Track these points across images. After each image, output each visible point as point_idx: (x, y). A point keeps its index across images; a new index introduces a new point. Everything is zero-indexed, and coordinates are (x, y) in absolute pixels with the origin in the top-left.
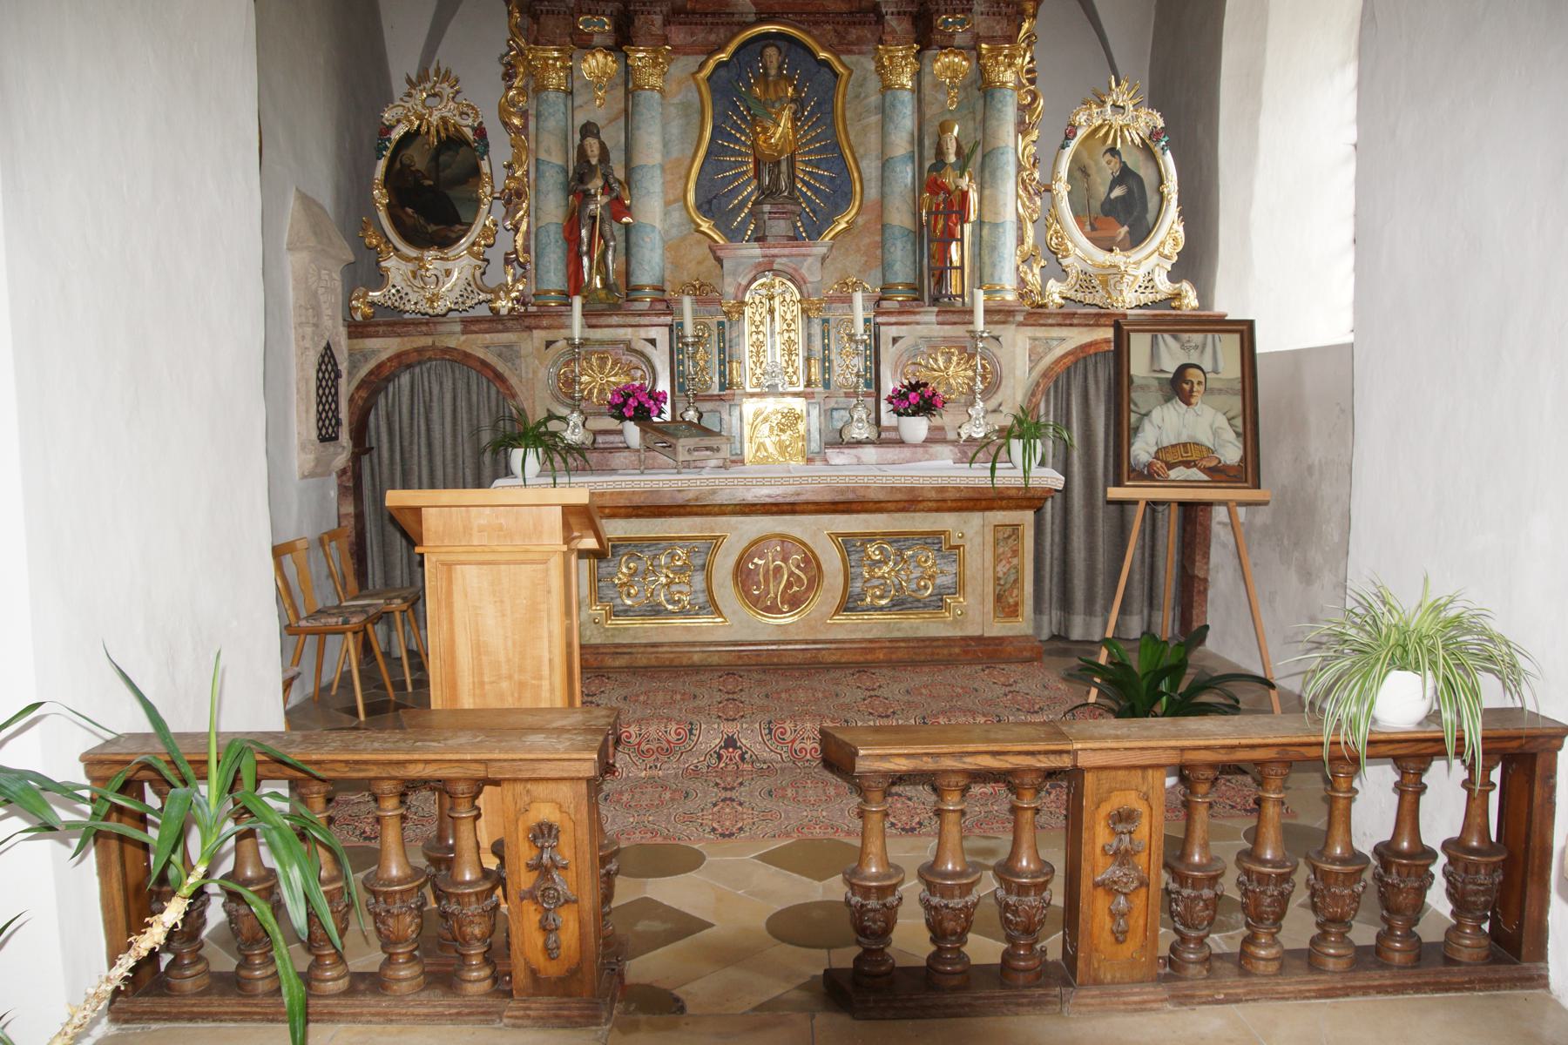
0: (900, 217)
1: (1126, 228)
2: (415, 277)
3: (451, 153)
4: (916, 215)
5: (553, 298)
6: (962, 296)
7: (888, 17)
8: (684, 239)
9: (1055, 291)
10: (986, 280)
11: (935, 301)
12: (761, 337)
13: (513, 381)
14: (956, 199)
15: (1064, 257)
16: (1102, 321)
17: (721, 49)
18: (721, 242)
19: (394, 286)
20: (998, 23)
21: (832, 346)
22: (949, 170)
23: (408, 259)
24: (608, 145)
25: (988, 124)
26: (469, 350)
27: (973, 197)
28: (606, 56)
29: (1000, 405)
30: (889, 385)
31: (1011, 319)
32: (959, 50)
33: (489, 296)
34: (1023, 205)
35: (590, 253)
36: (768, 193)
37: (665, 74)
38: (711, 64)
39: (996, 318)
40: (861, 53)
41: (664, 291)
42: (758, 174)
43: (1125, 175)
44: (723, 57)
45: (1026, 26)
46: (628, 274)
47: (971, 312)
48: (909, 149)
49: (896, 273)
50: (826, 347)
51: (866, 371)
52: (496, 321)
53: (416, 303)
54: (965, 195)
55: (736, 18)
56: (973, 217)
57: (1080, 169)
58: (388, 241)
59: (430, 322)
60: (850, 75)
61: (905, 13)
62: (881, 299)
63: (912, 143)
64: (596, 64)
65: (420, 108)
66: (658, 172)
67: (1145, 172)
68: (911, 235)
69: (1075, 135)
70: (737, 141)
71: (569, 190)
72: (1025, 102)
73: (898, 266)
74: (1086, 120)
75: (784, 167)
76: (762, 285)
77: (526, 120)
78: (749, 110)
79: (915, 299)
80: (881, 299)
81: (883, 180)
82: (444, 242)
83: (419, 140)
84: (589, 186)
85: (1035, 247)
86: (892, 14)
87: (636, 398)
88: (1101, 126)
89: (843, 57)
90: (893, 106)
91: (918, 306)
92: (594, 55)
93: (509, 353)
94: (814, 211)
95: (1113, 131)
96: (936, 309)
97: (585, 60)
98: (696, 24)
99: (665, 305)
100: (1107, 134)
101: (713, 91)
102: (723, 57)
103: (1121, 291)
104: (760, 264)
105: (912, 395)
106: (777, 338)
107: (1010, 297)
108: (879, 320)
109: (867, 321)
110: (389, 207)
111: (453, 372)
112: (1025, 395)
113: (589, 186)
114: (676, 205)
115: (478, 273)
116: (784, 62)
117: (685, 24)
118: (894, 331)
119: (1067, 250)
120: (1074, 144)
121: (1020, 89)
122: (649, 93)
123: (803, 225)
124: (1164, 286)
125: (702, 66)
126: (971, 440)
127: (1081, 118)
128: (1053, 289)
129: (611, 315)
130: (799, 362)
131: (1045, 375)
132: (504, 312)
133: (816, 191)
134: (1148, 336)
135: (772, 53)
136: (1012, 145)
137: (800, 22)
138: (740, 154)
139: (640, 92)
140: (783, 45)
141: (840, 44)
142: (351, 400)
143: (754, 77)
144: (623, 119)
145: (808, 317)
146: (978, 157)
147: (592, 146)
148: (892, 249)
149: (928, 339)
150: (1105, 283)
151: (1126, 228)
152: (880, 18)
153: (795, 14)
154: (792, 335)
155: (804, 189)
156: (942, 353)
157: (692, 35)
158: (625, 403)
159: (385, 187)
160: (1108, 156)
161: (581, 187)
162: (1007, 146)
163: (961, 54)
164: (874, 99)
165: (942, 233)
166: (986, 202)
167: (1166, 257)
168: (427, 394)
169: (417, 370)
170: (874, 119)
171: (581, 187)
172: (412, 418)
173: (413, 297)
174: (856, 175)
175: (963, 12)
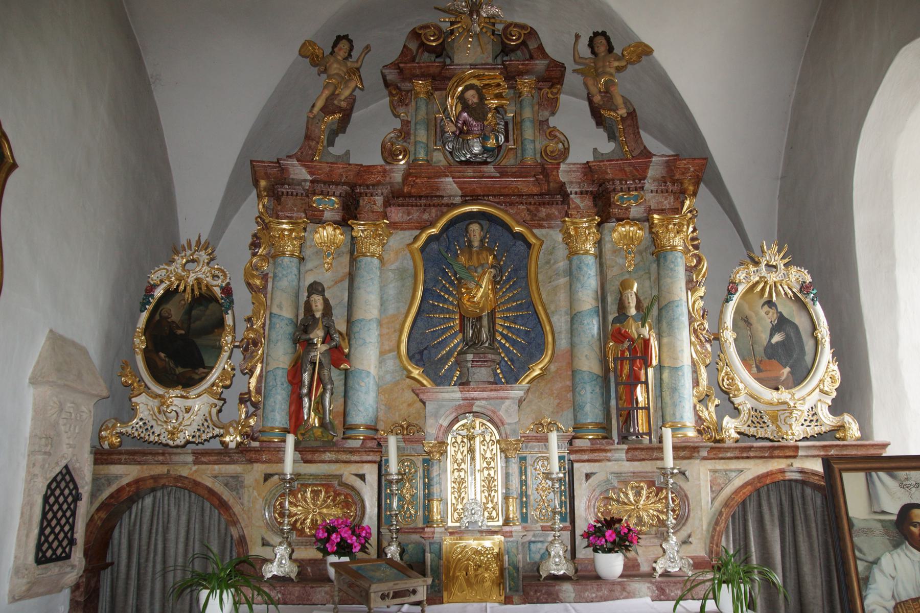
0: (588, 363)
1: (788, 369)
2: (160, 412)
3: (201, 308)
4: (604, 362)
5: (276, 434)
6: (649, 434)
7: (572, 196)
8: (397, 383)
10: (668, 418)
11: (624, 439)
12: (462, 474)
13: (237, 509)
14: (639, 345)
15: (735, 396)
16: (776, 453)
17: (432, 224)
18: (429, 386)
19: (141, 419)
20: (666, 199)
21: (529, 482)
22: (631, 321)
23: (157, 396)
24: (332, 302)
25: (662, 282)
26: (199, 479)
27: (654, 343)
28: (335, 229)
29: (689, 536)
30: (586, 516)
31: (696, 454)
32: (634, 221)
33: (222, 431)
34: (696, 351)
35: (309, 394)
36: (472, 344)
37: (384, 245)
38: (424, 237)
39: (682, 454)
40: (550, 227)
41: (377, 430)
42: (462, 329)
43: (782, 323)
44: (434, 231)
45: (687, 203)
46: (345, 414)
47: (661, 449)
48: (594, 303)
49: (586, 414)
50: (523, 483)
51: (561, 507)
52: (224, 454)
53: (159, 435)
54: (646, 342)
55: (445, 200)
56: (655, 362)
57: (742, 319)
58: (141, 380)
59: (163, 451)
60: (542, 243)
61: (587, 192)
62: (574, 438)
63: (597, 299)
64: (326, 233)
65: (180, 271)
66: (374, 326)
67: (800, 321)
68: (600, 380)
69: (737, 290)
70: (445, 301)
71: (296, 341)
72: (693, 264)
73: (588, 408)
74: (745, 277)
75: (485, 322)
76: (463, 425)
77: (267, 281)
78: (455, 274)
79: (604, 438)
80: (574, 438)
81: (572, 331)
82: (188, 383)
83: (177, 298)
84: (312, 336)
85: (709, 387)
86: (576, 193)
87: (338, 533)
88: (757, 283)
89: (535, 231)
90: (580, 268)
91: (608, 444)
92: (324, 228)
93: (235, 484)
94: (512, 360)
95: (768, 286)
96: (625, 447)
97: (316, 232)
98: (412, 206)
100: (763, 289)
101: (425, 260)
102: (434, 231)
103: (790, 425)
104: (460, 406)
105: (608, 533)
106: (478, 475)
108: (572, 457)
109: (561, 458)
110: (146, 352)
111: (190, 496)
112: (709, 524)
113: (312, 336)
114: (391, 355)
115: (214, 411)
116: (485, 237)
117: (403, 205)
118: (587, 468)
119: (739, 390)
120: (736, 298)
121: (686, 254)
122: (369, 258)
123: (502, 372)
124: (828, 420)
125: (416, 239)
126: (666, 574)
127: (741, 276)
128: (729, 425)
129: (324, 452)
130: (499, 497)
131: (726, 504)
132: (232, 445)
133: (514, 343)
134: (861, 475)
135: (475, 229)
137: (498, 203)
138: (448, 312)
139: (361, 258)
140: (485, 223)
141: (532, 220)
142: (90, 523)
143: (460, 249)
144: (346, 284)
145: (506, 457)
146: (655, 312)
147: (318, 303)
148: (582, 392)
149: (618, 475)
150: (775, 419)
151: (788, 369)
152: (566, 196)
153: (494, 196)
154: (492, 472)
155: (503, 341)
156: (632, 488)
157: (409, 214)
158: (328, 539)
159: (145, 334)
160: (766, 308)
161: (304, 337)
162: (681, 300)
163: (635, 224)
164: (562, 264)
165: (629, 377)
166: (665, 349)
167: (826, 393)
168: (166, 516)
169: (159, 494)
170: (563, 281)
171: (304, 337)
172: (150, 538)
173: (157, 430)
174: (548, 328)
175: (636, 190)
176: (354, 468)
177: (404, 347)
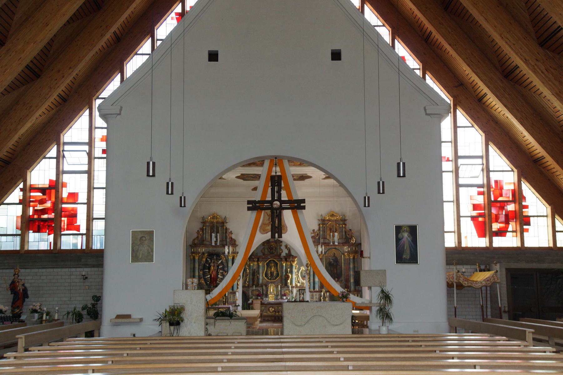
9: (299, 285)
17: (267, 261)
27: (290, 276)
54: (289, 276)
56: (290, 278)
64: (256, 263)
99: (262, 286)
127: (301, 268)
136: (295, 271)
177: (264, 276)
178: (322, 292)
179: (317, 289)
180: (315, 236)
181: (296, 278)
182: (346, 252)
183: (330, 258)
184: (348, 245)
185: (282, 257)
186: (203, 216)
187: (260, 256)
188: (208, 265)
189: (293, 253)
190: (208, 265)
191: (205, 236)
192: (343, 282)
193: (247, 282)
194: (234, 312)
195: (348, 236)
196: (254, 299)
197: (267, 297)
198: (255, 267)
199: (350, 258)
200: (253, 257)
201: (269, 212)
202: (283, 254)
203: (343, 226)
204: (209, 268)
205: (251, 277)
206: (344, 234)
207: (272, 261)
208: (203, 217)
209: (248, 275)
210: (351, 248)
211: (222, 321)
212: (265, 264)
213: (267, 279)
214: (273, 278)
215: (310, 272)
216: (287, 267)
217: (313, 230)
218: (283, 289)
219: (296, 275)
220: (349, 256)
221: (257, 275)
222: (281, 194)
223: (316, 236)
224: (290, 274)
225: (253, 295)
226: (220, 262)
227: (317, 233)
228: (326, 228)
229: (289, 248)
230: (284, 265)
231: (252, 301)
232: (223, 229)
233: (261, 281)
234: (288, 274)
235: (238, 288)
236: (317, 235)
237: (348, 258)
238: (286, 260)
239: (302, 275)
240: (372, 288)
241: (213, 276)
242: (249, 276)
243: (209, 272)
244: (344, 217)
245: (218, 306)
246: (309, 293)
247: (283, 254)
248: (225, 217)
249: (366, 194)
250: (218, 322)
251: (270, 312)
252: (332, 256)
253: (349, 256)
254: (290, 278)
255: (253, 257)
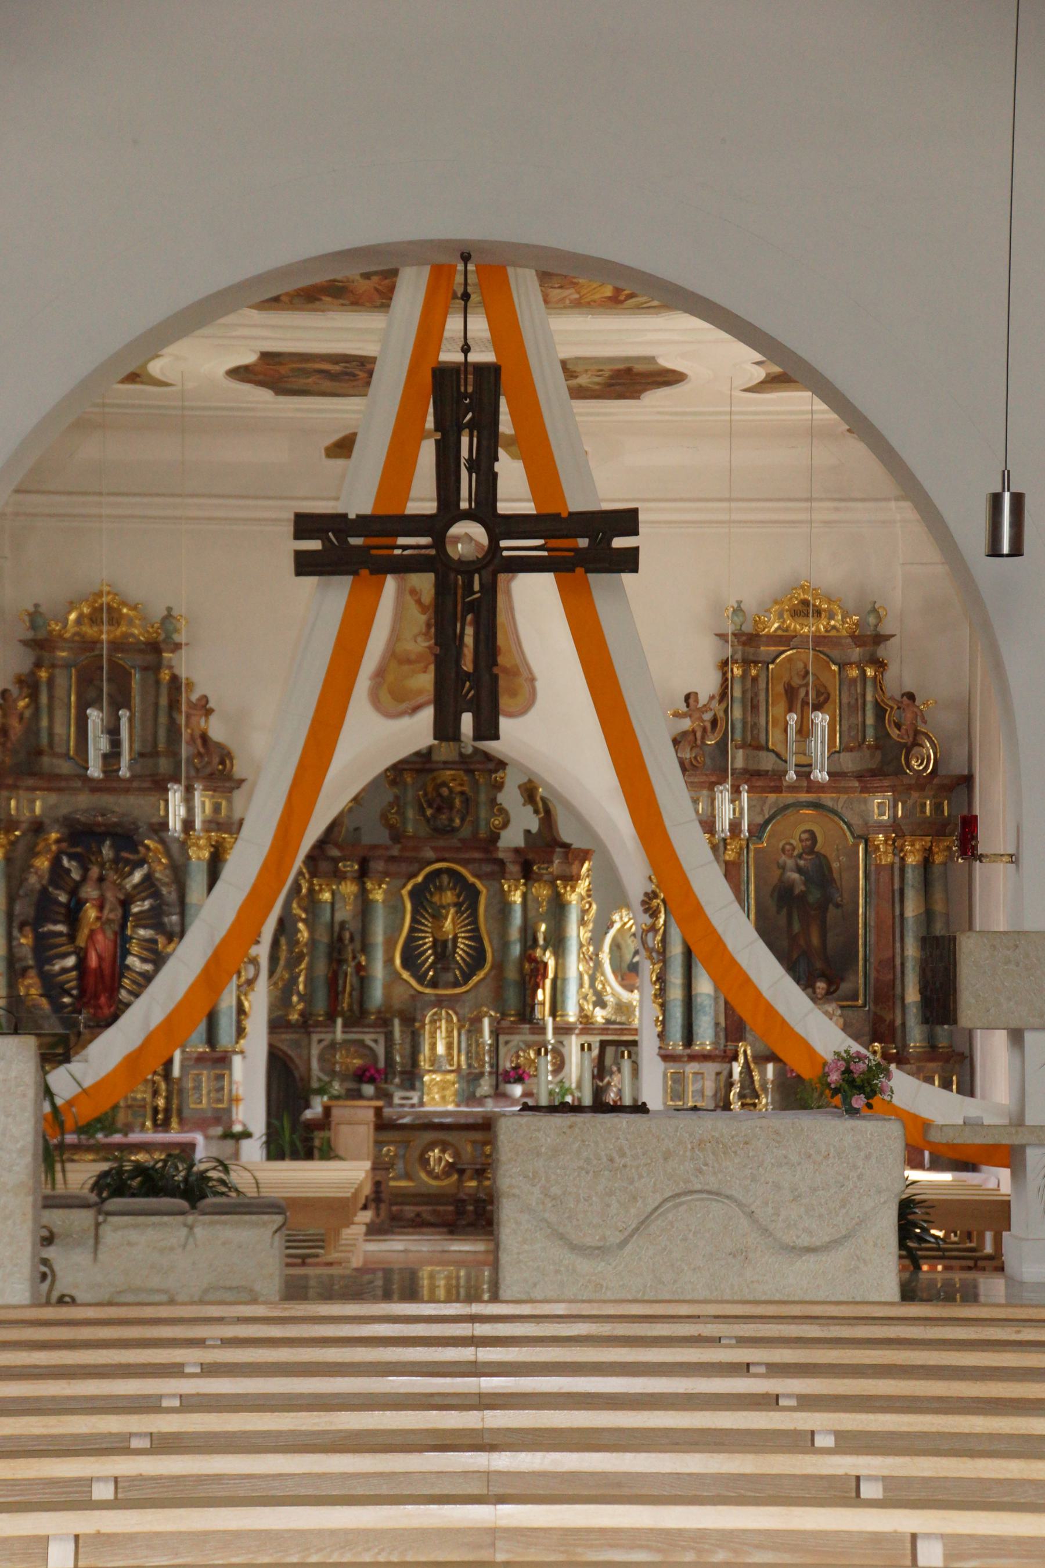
7: (508, 864)
9: (600, 1015)
16: (625, 1032)
17: (414, 875)
27: (551, 963)
54: (546, 965)
56: (551, 974)
64: (349, 888)
99: (384, 1022)
107: (572, 1019)
125: (404, 886)
127: (616, 917)
136: (576, 933)
149: (525, 1042)
176: (373, 1036)
177: (398, 961)
178: (735, 1058)
179: (706, 1039)
180: (699, 735)
181: (586, 978)
182: (881, 827)
183: (783, 858)
184: (893, 789)
185: (501, 855)
186: (36, 606)
187: (374, 847)
188: (63, 898)
189: (567, 833)
190: (63, 898)
191: (44, 723)
192: (860, 1002)
193: (295, 999)
194: (214, 1168)
195: (894, 733)
196: (337, 1098)
197: (412, 1088)
198: (345, 912)
199: (903, 859)
200: (335, 852)
201: (424, 582)
202: (512, 838)
203: (864, 672)
204: (73, 915)
205: (322, 968)
206: (870, 720)
207: (445, 879)
208: (31, 609)
209: (300, 957)
210: (910, 802)
211: (141, 1219)
212: (405, 892)
213: (413, 983)
214: (449, 977)
215: (664, 940)
216: (531, 914)
217: (687, 698)
218: (507, 1043)
219: (583, 958)
220: (898, 850)
221: (354, 958)
222: (495, 476)
223: (704, 730)
224: (548, 954)
225: (333, 1074)
226: (137, 876)
227: (708, 716)
228: (762, 685)
229: (543, 799)
230: (517, 898)
231: (327, 1110)
232: (158, 682)
233: (377, 994)
234: (538, 952)
235: (241, 1032)
236: (708, 725)
237: (892, 865)
238: (527, 874)
239: (621, 957)
240: (1029, 1037)
241: (93, 961)
242: (310, 968)
243: (72, 937)
244: (872, 620)
245: (126, 1135)
246: (660, 1065)
247: (512, 838)
248: (165, 613)
249: (1006, 477)
250: (116, 1229)
251: (430, 1173)
252: (796, 853)
253: (898, 850)
254: (551, 974)
255: (335, 852)
